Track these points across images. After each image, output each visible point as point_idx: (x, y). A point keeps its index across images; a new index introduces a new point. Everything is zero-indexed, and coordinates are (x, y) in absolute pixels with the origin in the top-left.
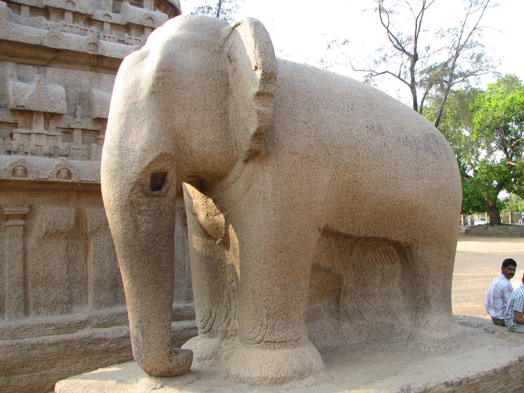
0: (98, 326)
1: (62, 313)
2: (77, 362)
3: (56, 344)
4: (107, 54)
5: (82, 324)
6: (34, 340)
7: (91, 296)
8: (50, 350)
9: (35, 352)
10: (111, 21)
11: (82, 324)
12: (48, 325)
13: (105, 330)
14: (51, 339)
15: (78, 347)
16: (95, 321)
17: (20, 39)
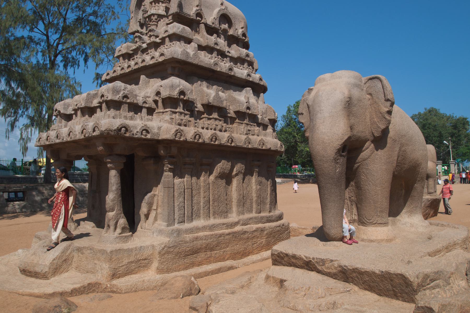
0: (243, 225)
1: (225, 218)
2: (237, 244)
3: (229, 234)
4: (237, 75)
5: (236, 224)
6: (221, 232)
7: (234, 209)
8: (227, 237)
9: (221, 238)
10: (230, 55)
11: (236, 224)
12: (224, 224)
13: (246, 227)
14: (227, 231)
15: (237, 236)
16: (241, 223)
17: (202, 64)
